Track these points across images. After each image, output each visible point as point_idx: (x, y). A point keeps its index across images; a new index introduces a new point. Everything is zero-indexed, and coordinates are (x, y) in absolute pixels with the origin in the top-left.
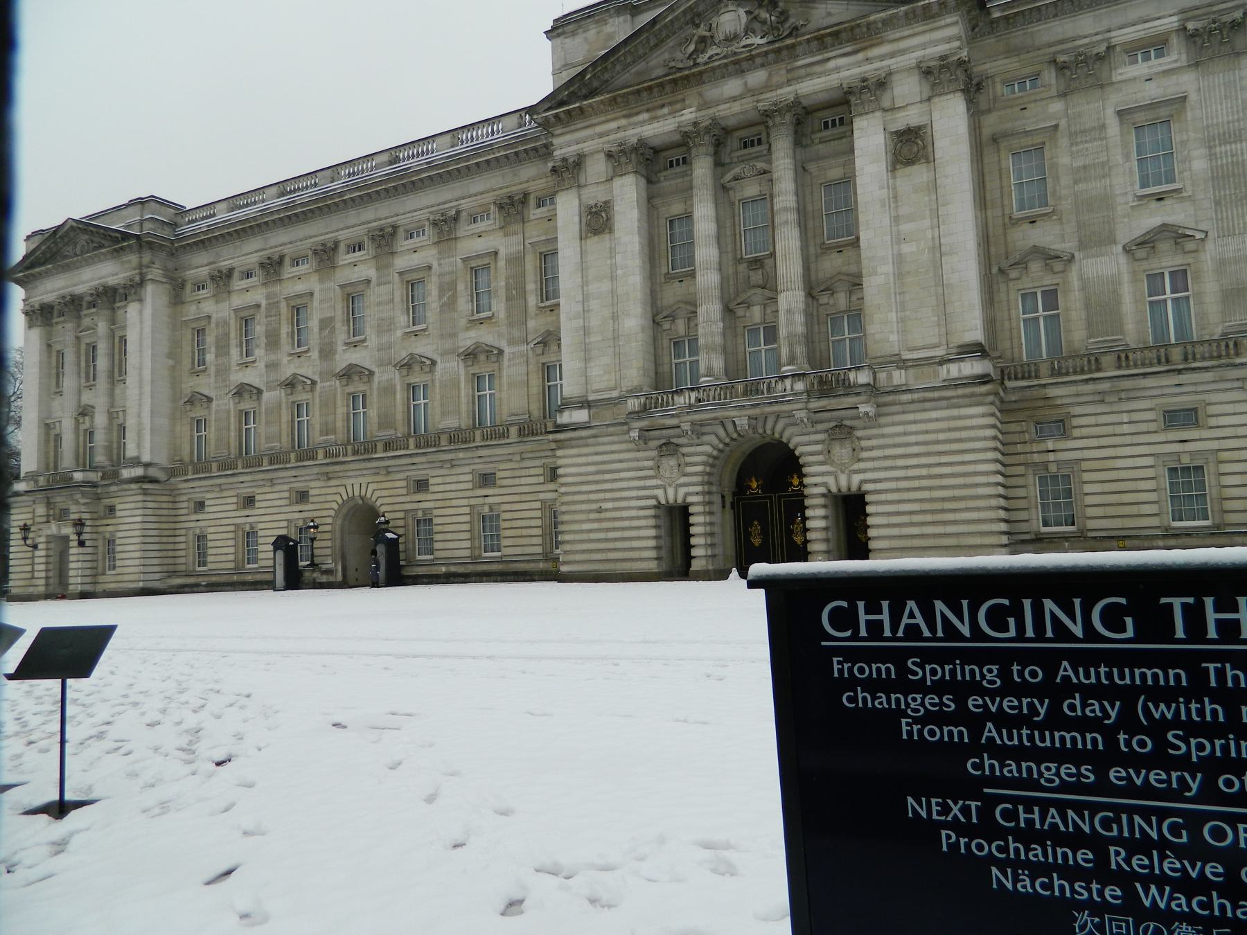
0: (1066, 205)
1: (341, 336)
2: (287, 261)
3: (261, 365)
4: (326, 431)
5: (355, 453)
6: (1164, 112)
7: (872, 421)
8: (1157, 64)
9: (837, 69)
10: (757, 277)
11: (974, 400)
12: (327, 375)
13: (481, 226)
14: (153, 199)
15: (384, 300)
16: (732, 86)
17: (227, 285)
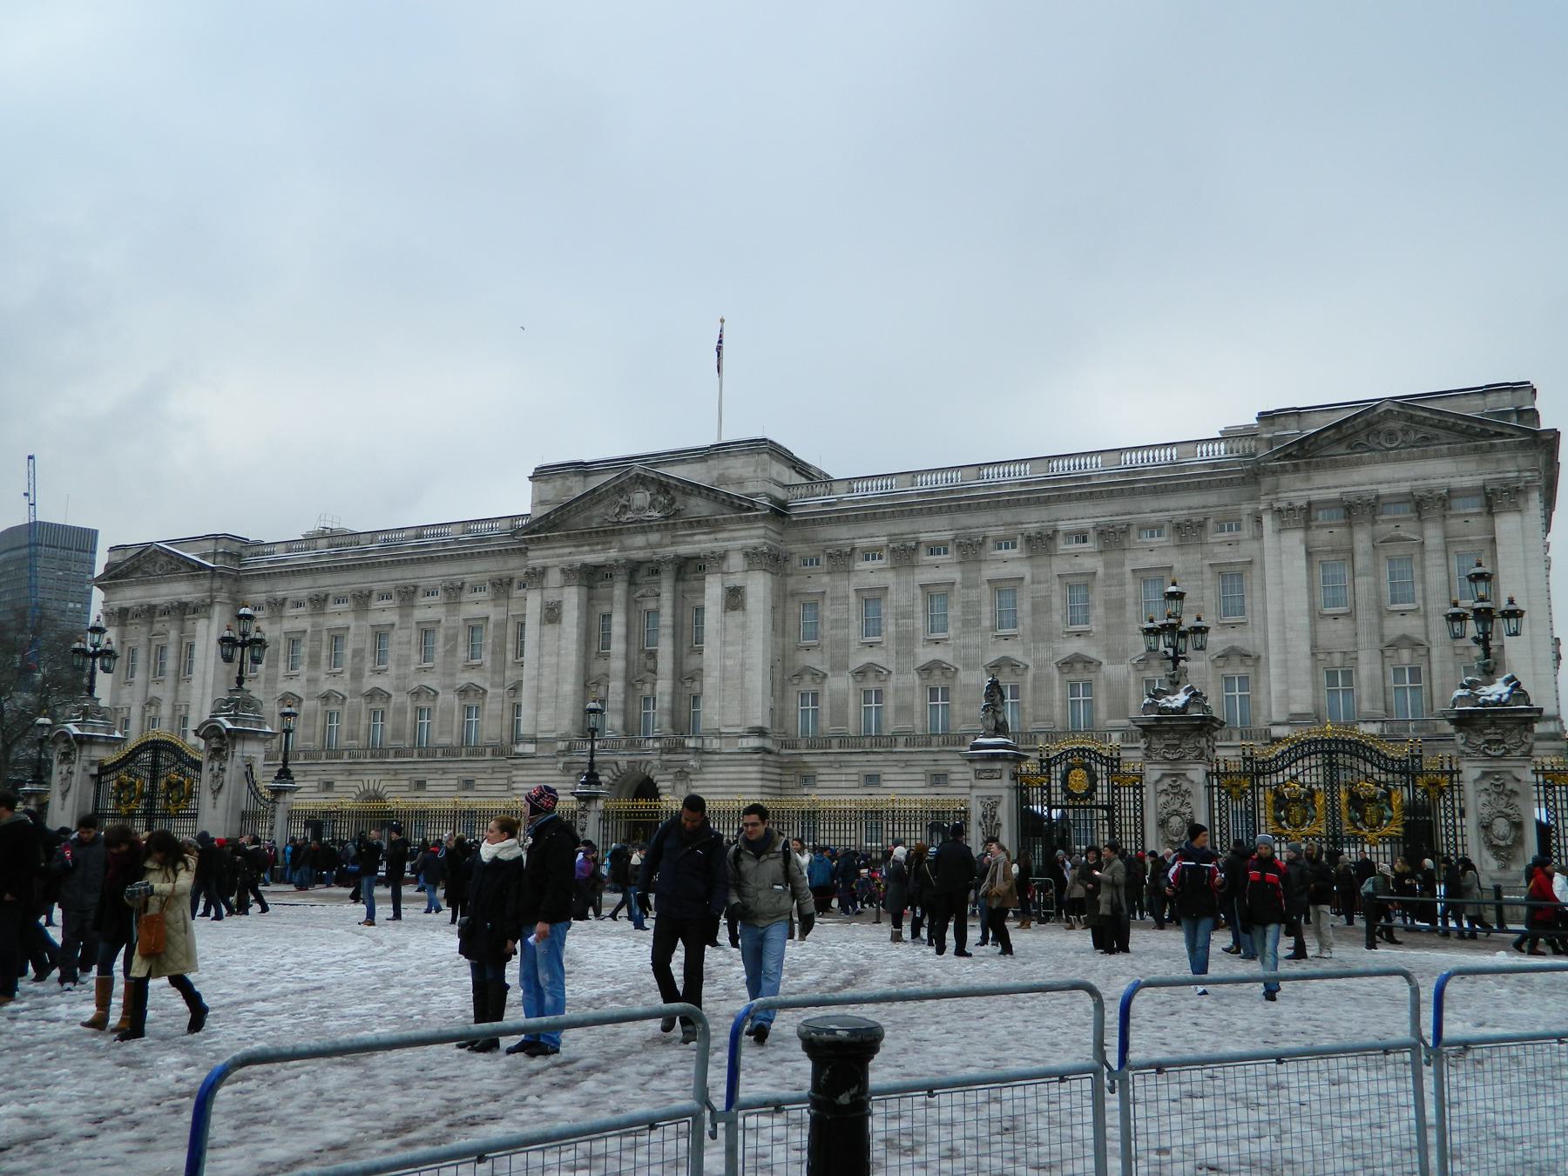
0: (826, 642)
1: (368, 665)
2: (331, 598)
3: (303, 679)
4: (352, 736)
5: (373, 756)
6: (877, 594)
7: (699, 771)
8: (878, 563)
9: (699, 542)
10: (650, 664)
11: (751, 763)
12: (355, 693)
13: (479, 595)
14: (226, 537)
15: (403, 642)
16: (639, 540)
17: (280, 611)
